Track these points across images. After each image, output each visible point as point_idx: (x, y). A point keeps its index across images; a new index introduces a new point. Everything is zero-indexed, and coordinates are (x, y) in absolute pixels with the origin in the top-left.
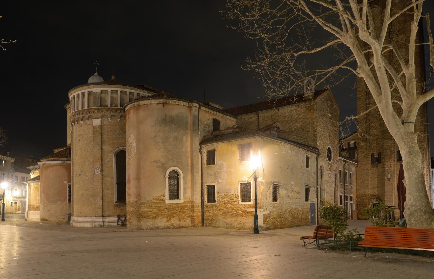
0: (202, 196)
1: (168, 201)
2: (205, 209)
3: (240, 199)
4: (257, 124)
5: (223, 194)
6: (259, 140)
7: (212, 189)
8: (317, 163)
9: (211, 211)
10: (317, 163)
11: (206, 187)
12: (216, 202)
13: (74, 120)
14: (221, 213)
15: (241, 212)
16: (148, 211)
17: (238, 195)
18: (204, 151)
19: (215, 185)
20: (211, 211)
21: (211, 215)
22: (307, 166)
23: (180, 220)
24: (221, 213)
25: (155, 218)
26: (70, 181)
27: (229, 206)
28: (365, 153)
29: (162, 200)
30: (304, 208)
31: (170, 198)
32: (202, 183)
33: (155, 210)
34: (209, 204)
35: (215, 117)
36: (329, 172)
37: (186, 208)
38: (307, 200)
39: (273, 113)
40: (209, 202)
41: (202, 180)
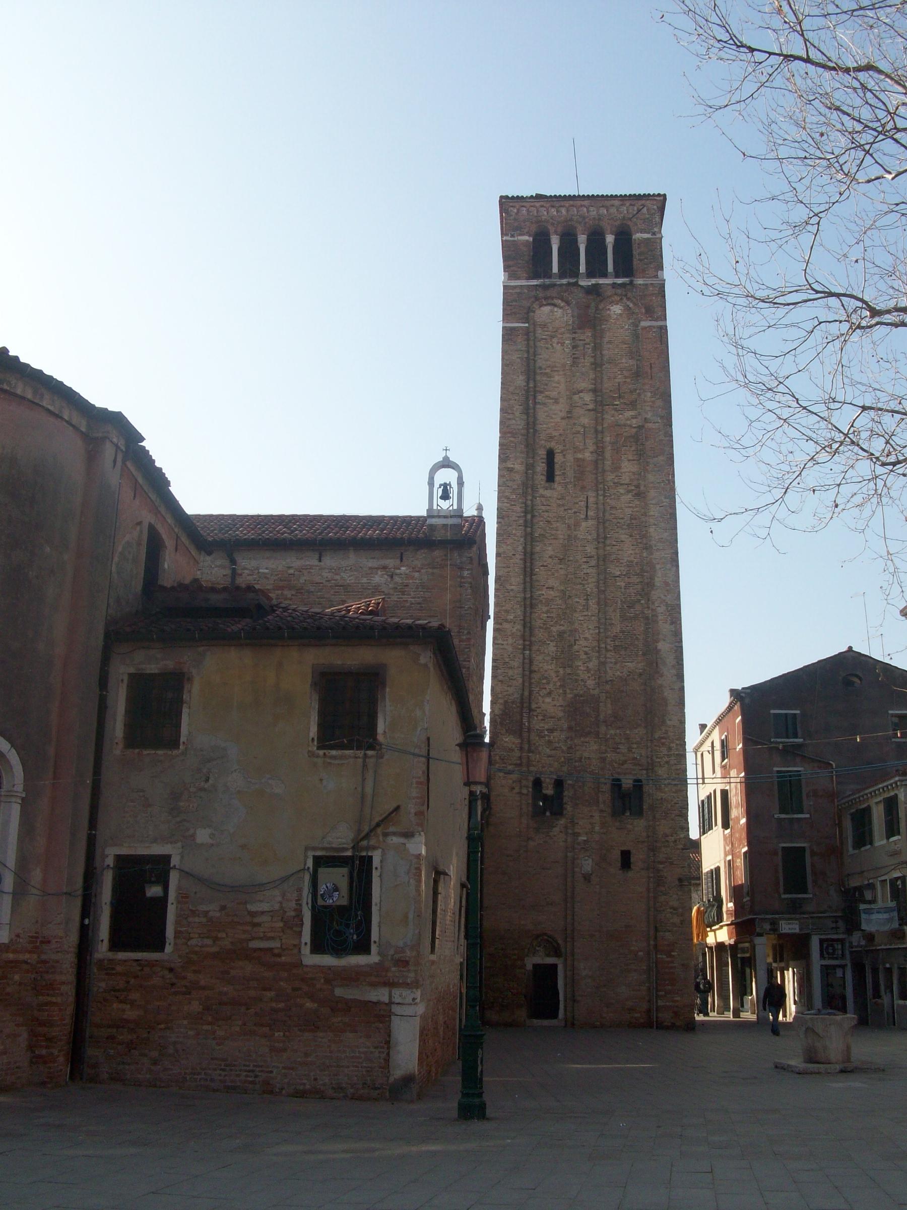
0: (88, 907)
2: (99, 985)
3: (306, 936)
9: (135, 996)
11: (110, 861)
12: (168, 949)
14: (196, 1007)
15: (309, 1005)
17: (299, 916)
18: (121, 671)
19: (167, 859)
20: (135, 996)
21: (131, 1014)
24: (196, 1007)
28: (515, 776)
32: (91, 842)
34: (122, 955)
40: (116, 944)
41: (93, 823)
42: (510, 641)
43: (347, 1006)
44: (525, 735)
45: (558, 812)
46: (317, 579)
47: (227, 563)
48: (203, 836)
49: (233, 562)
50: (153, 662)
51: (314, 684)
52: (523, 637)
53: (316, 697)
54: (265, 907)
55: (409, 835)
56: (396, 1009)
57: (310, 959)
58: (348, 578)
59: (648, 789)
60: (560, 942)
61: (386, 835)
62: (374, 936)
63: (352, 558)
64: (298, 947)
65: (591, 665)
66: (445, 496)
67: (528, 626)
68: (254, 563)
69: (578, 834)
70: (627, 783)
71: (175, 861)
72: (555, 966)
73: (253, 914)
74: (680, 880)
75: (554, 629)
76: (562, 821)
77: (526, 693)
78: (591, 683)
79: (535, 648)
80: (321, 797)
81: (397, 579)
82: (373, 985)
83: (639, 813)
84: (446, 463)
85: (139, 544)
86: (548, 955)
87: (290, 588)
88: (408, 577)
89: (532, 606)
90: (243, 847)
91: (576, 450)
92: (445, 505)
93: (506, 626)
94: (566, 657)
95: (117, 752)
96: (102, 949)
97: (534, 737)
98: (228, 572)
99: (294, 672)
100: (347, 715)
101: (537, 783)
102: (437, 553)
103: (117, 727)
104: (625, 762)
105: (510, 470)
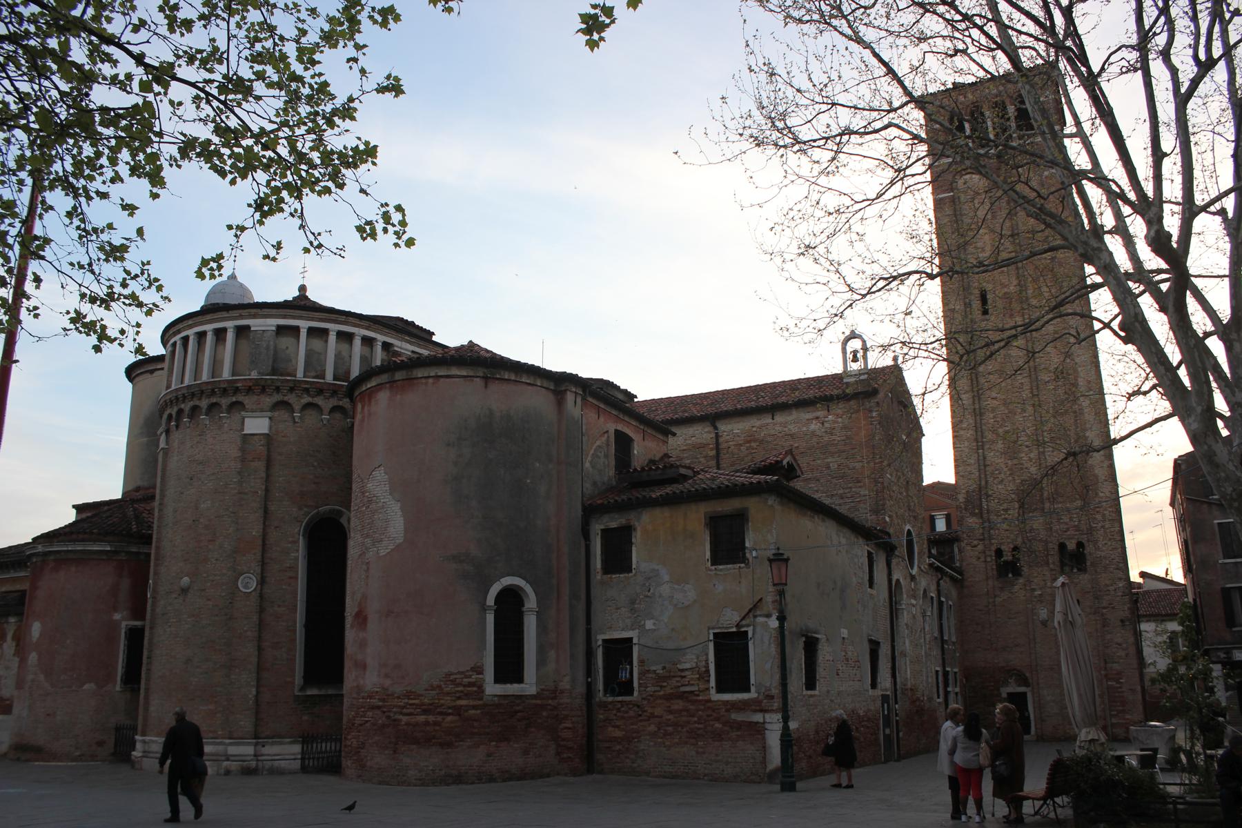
0: (589, 671)
1: (492, 689)
3: (713, 683)
4: (714, 453)
5: (660, 667)
6: (770, 502)
7: (619, 650)
8: (890, 574)
10: (890, 574)
11: (600, 643)
12: (636, 694)
13: (180, 412)
14: (653, 728)
15: (718, 725)
16: (427, 723)
17: (708, 671)
18: (597, 528)
22: (871, 585)
23: (526, 752)
24: (653, 728)
25: (449, 745)
26: (138, 610)
27: (678, 705)
29: (471, 684)
30: (869, 710)
31: (497, 680)
33: (449, 718)
35: (619, 428)
36: (913, 602)
37: (544, 714)
38: (874, 685)
39: (758, 423)
42: (966, 444)
43: (739, 725)
44: (985, 516)
45: (1017, 572)
46: (773, 432)
47: (711, 429)
48: (649, 624)
49: (716, 428)
50: (614, 522)
51: (706, 525)
52: (976, 440)
53: (708, 532)
54: (688, 666)
55: (769, 616)
56: (767, 726)
57: (716, 697)
58: (793, 428)
59: (1089, 549)
60: (1028, 675)
61: (755, 617)
62: (752, 681)
63: (794, 415)
64: (708, 689)
65: (1032, 455)
66: (855, 360)
67: (978, 428)
68: (730, 427)
69: (1034, 590)
70: (1071, 545)
71: (635, 641)
72: (1025, 694)
73: (682, 670)
74: (1122, 621)
75: (1000, 430)
76: (1021, 580)
77: (983, 483)
78: (1033, 470)
79: (987, 447)
80: (727, 595)
81: (827, 425)
82: (755, 711)
83: (1083, 570)
84: (853, 335)
85: (608, 445)
86: (1019, 686)
87: (755, 441)
88: (835, 422)
89: (981, 414)
90: (673, 629)
91: (1003, 286)
92: (855, 366)
93: (962, 432)
94: (1012, 451)
95: (599, 577)
96: (600, 695)
97: (993, 517)
98: (713, 435)
99: (695, 518)
100: (728, 545)
101: (999, 553)
102: (852, 403)
103: (598, 563)
104: (1068, 530)
105: (953, 311)
